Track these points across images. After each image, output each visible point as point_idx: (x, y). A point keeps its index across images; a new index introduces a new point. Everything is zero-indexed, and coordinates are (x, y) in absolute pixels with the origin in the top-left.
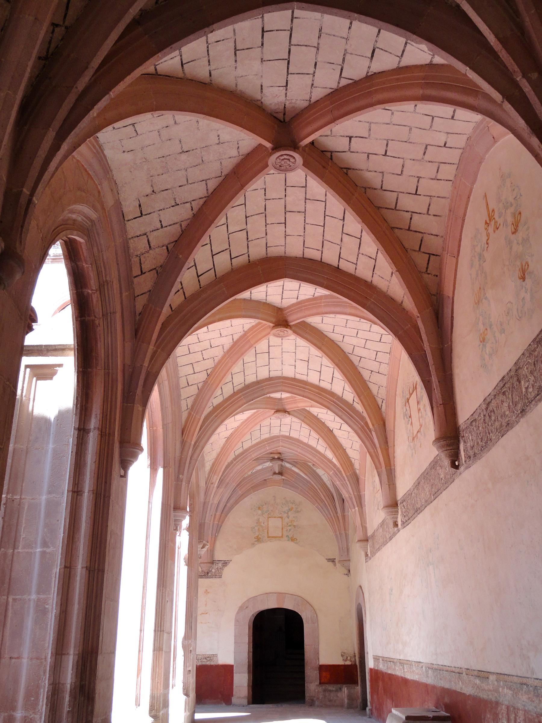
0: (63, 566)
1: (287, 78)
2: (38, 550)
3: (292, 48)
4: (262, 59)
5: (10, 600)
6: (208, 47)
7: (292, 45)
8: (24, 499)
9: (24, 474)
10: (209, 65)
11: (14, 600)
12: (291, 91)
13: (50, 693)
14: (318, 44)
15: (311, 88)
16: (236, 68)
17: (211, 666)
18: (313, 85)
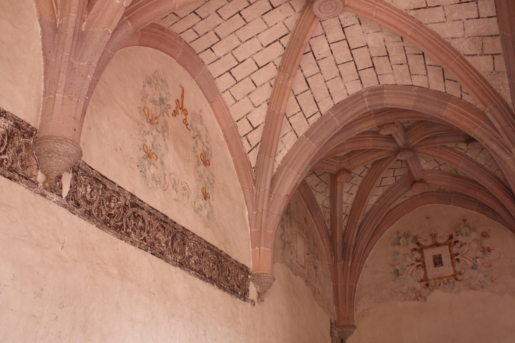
1: (345, 36)
3: (352, 59)
4: (368, 47)
6: (407, 61)
7: (352, 61)
10: (404, 47)
12: (337, 25)
14: (338, 68)
15: (325, 33)
16: (384, 41)
18: (326, 35)
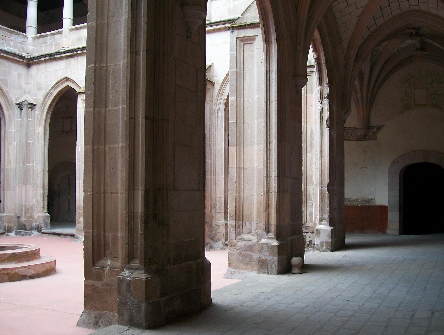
0: (128, 118)
2: (121, 107)
5: (107, 149)
8: (109, 66)
9: (107, 45)
11: (109, 148)
13: (127, 220)
17: (370, 207)
